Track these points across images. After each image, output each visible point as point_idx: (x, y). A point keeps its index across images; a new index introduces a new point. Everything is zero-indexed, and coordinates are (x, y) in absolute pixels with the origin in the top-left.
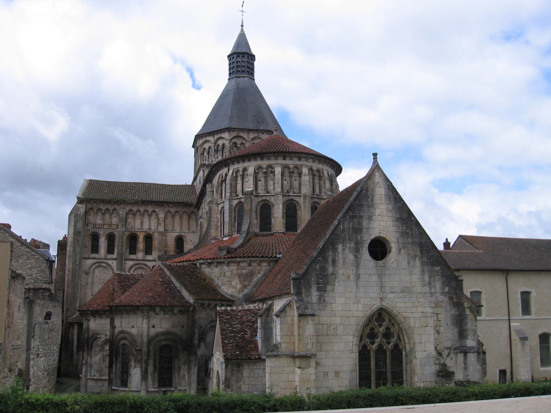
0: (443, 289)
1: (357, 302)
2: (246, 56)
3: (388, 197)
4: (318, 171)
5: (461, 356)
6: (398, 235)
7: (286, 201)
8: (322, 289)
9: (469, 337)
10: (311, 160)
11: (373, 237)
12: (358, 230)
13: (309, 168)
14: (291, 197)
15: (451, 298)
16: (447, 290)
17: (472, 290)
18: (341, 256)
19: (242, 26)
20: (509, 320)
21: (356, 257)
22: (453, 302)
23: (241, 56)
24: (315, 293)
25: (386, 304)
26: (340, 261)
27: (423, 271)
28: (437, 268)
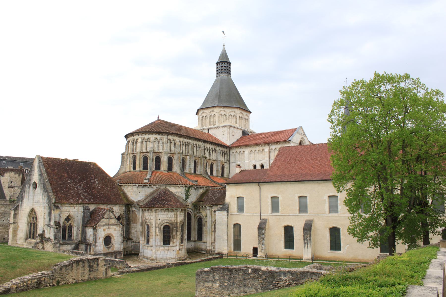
0: (47, 201)
1: (28, 206)
2: (221, 63)
3: (38, 167)
4: (148, 139)
5: (49, 228)
6: (39, 181)
7: (133, 156)
8: (22, 201)
9: (52, 221)
10: (144, 135)
11: (33, 182)
12: (30, 180)
13: (143, 138)
14: (134, 154)
15: (49, 205)
16: (48, 202)
17: (237, 196)
18: (26, 189)
19: (224, 45)
20: (260, 215)
21: (29, 190)
22: (49, 207)
23: (218, 64)
24: (20, 202)
25: (34, 207)
26: (26, 192)
27: (43, 195)
28: (46, 193)
